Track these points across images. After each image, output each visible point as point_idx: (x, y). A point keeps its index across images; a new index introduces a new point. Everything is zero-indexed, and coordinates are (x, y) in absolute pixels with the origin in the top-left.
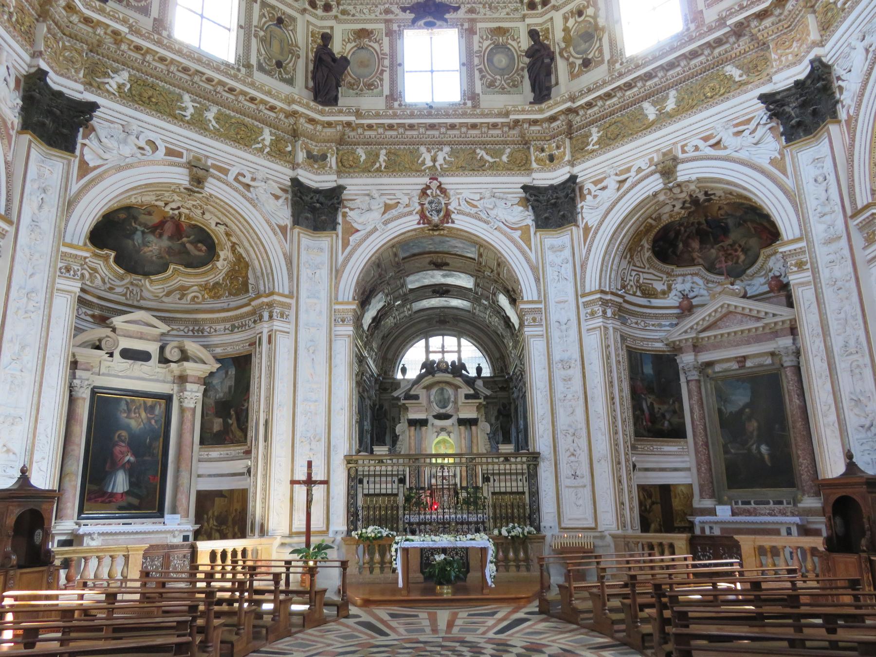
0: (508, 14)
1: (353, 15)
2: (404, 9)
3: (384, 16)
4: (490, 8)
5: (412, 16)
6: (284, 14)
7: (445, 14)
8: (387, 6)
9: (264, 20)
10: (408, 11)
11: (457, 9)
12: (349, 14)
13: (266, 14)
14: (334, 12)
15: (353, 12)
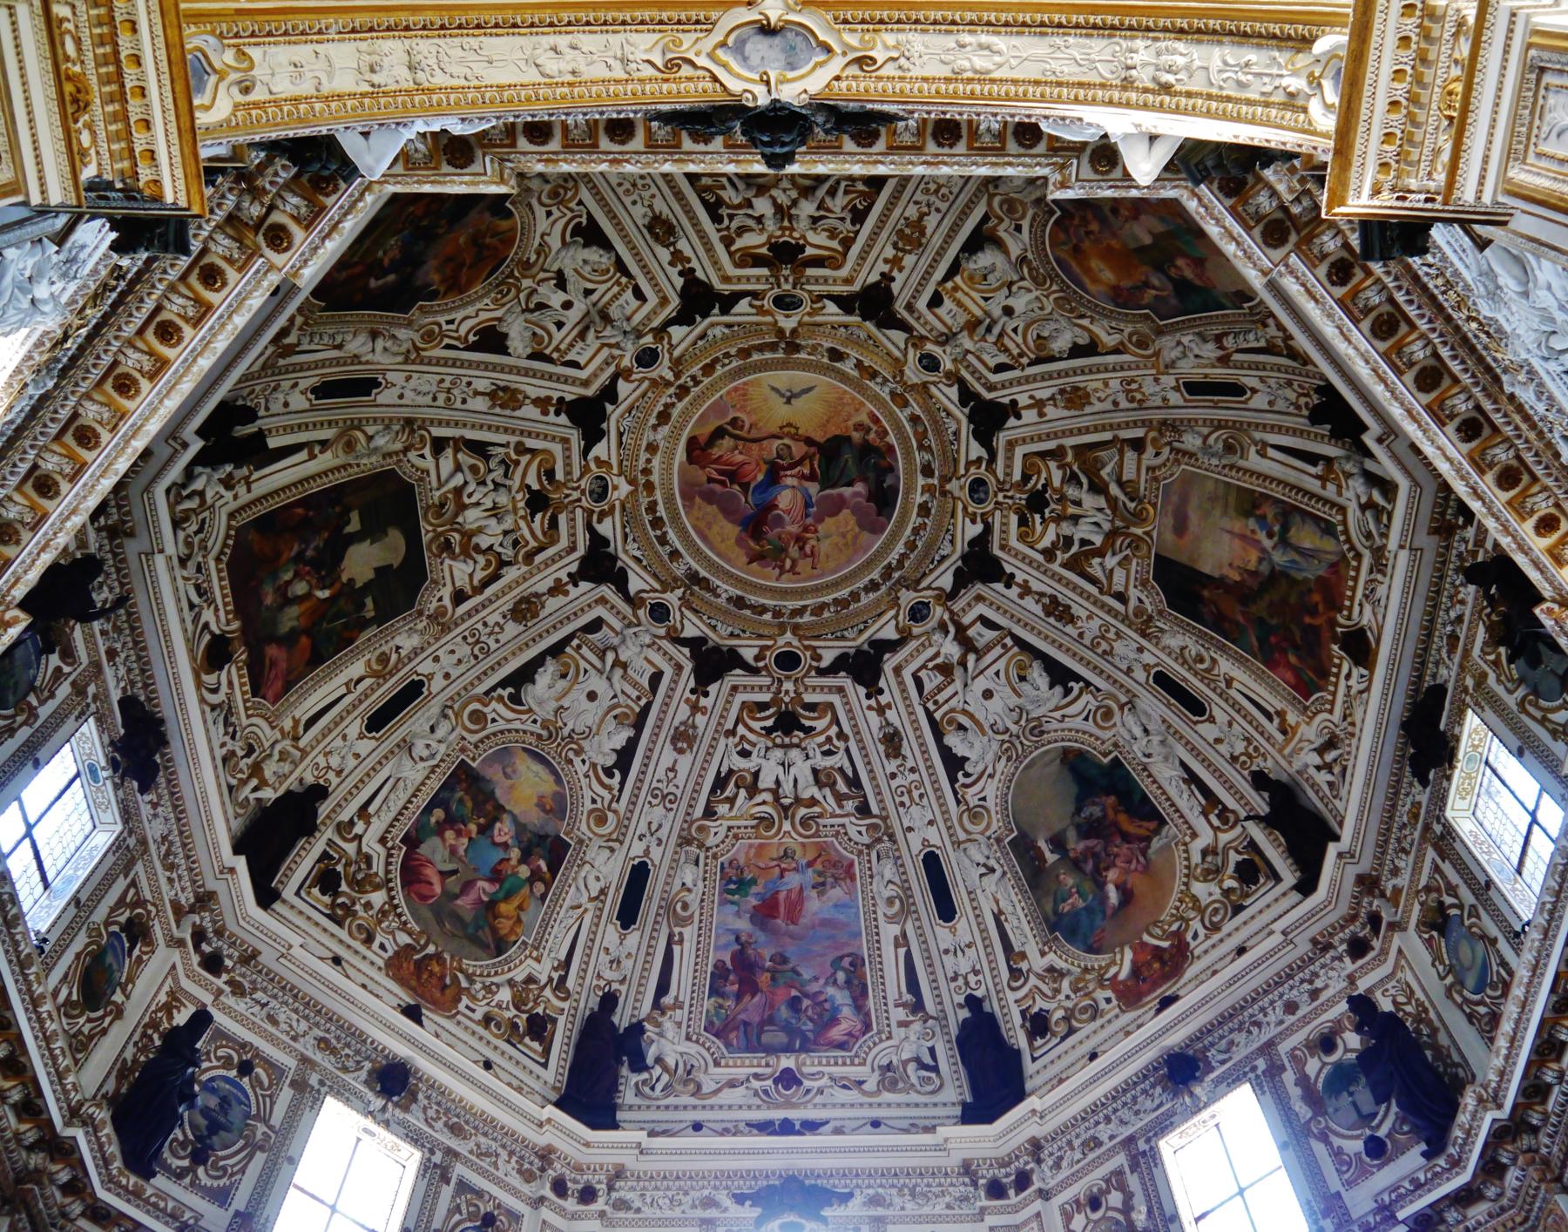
0: (949, 1206)
1: (638, 1210)
2: (740, 1199)
3: (700, 1213)
4: (913, 1195)
5: (757, 1211)
6: (499, 1206)
7: (822, 1208)
8: (706, 1192)
9: (457, 1217)
10: (748, 1203)
11: (846, 1198)
12: (629, 1208)
13: (463, 1207)
14: (600, 1204)
15: (637, 1204)
